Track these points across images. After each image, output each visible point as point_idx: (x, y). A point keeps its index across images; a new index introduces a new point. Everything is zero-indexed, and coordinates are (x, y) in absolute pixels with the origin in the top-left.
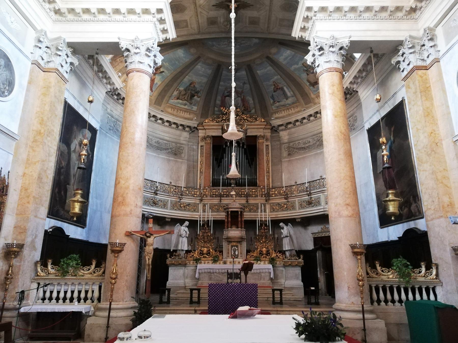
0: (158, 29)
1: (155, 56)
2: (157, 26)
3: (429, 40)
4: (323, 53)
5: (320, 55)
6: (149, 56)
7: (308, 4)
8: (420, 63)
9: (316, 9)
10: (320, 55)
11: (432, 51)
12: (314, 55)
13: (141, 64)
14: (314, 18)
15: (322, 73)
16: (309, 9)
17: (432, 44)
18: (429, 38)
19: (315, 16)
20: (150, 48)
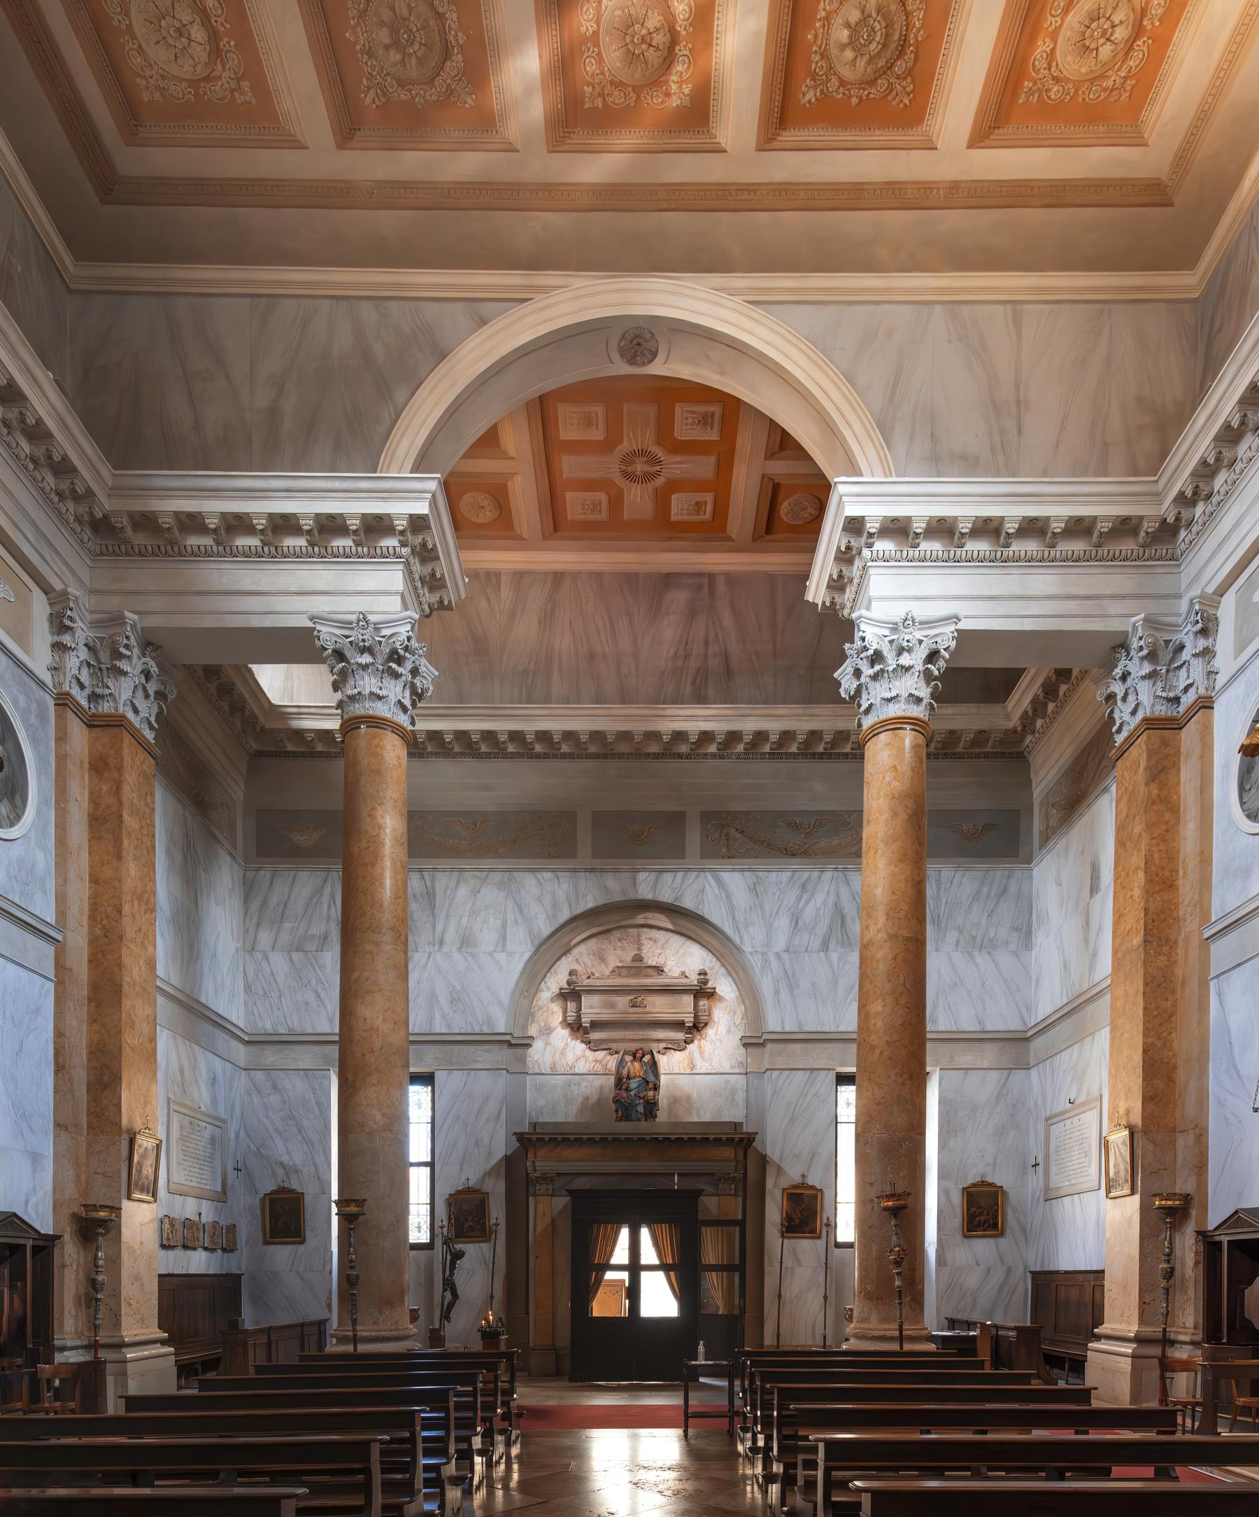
0: (417, 577)
1: (415, 672)
2: (414, 568)
3: (1196, 633)
4: (882, 671)
5: (875, 677)
6: (397, 676)
7: (852, 510)
8: (1162, 710)
9: (873, 527)
10: (875, 677)
11: (1197, 668)
12: (858, 673)
13: (379, 704)
14: (866, 553)
15: (875, 731)
16: (855, 526)
17: (1202, 643)
18: (1200, 626)
19: (870, 546)
20: (401, 652)
